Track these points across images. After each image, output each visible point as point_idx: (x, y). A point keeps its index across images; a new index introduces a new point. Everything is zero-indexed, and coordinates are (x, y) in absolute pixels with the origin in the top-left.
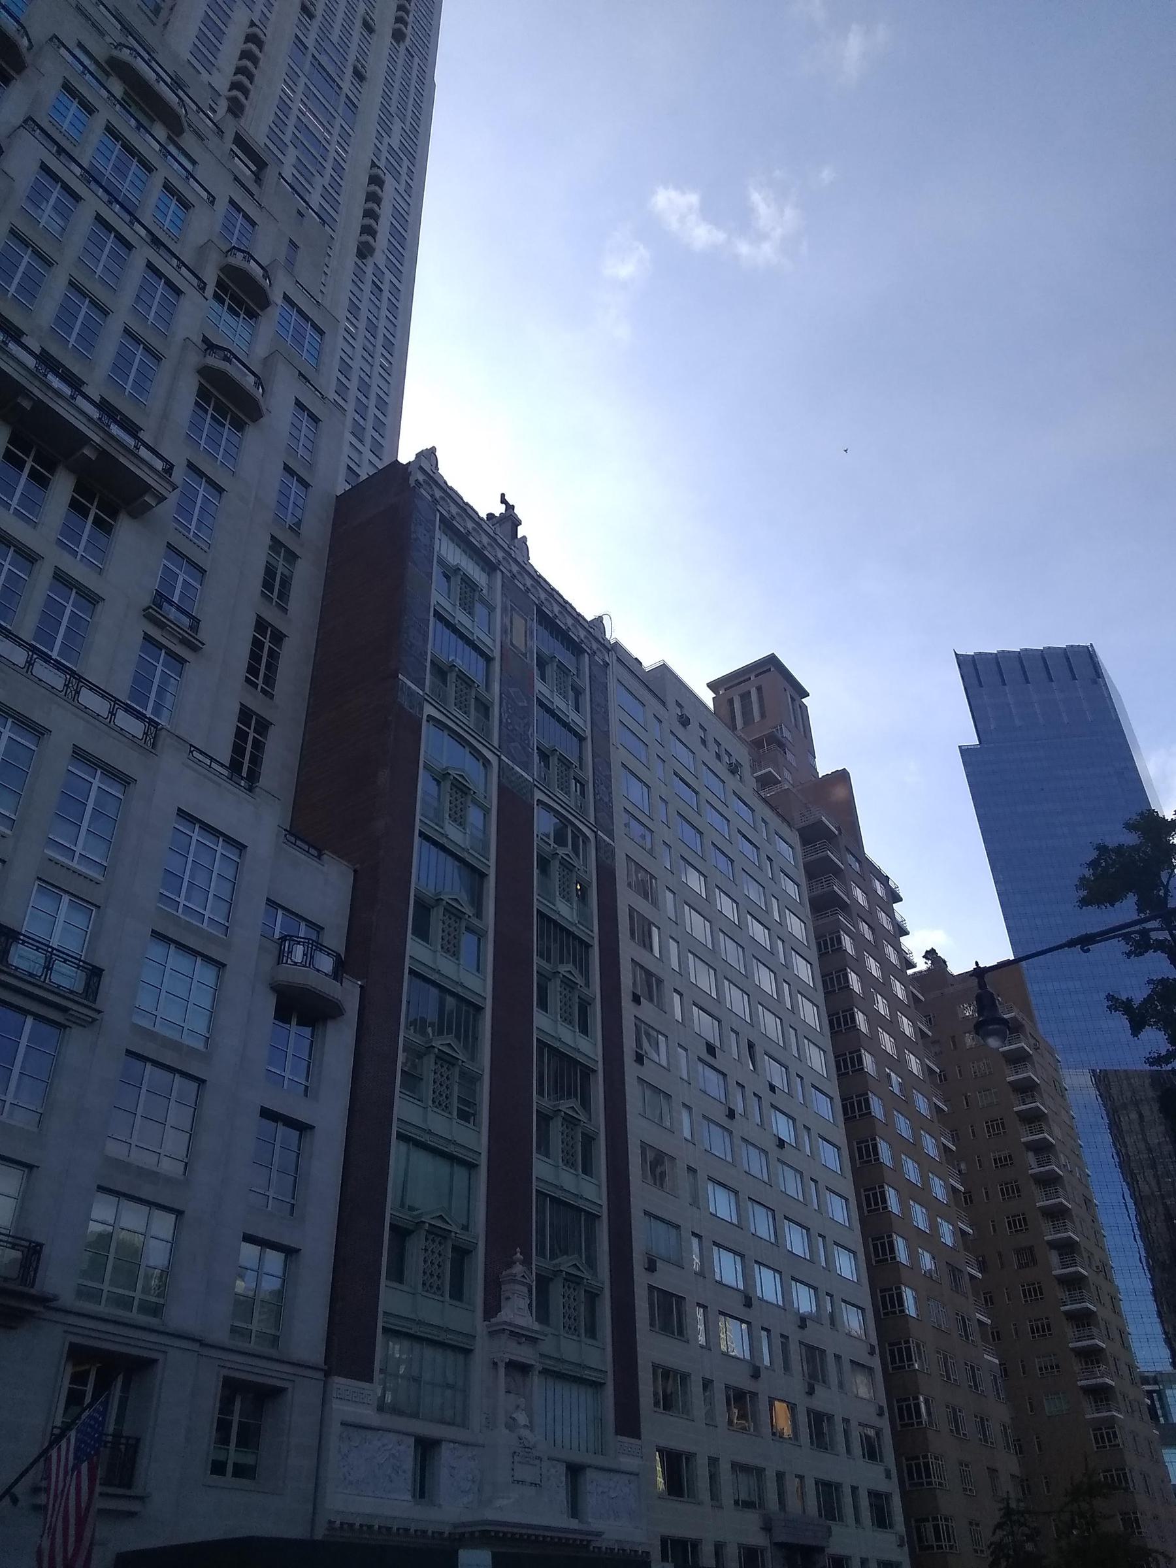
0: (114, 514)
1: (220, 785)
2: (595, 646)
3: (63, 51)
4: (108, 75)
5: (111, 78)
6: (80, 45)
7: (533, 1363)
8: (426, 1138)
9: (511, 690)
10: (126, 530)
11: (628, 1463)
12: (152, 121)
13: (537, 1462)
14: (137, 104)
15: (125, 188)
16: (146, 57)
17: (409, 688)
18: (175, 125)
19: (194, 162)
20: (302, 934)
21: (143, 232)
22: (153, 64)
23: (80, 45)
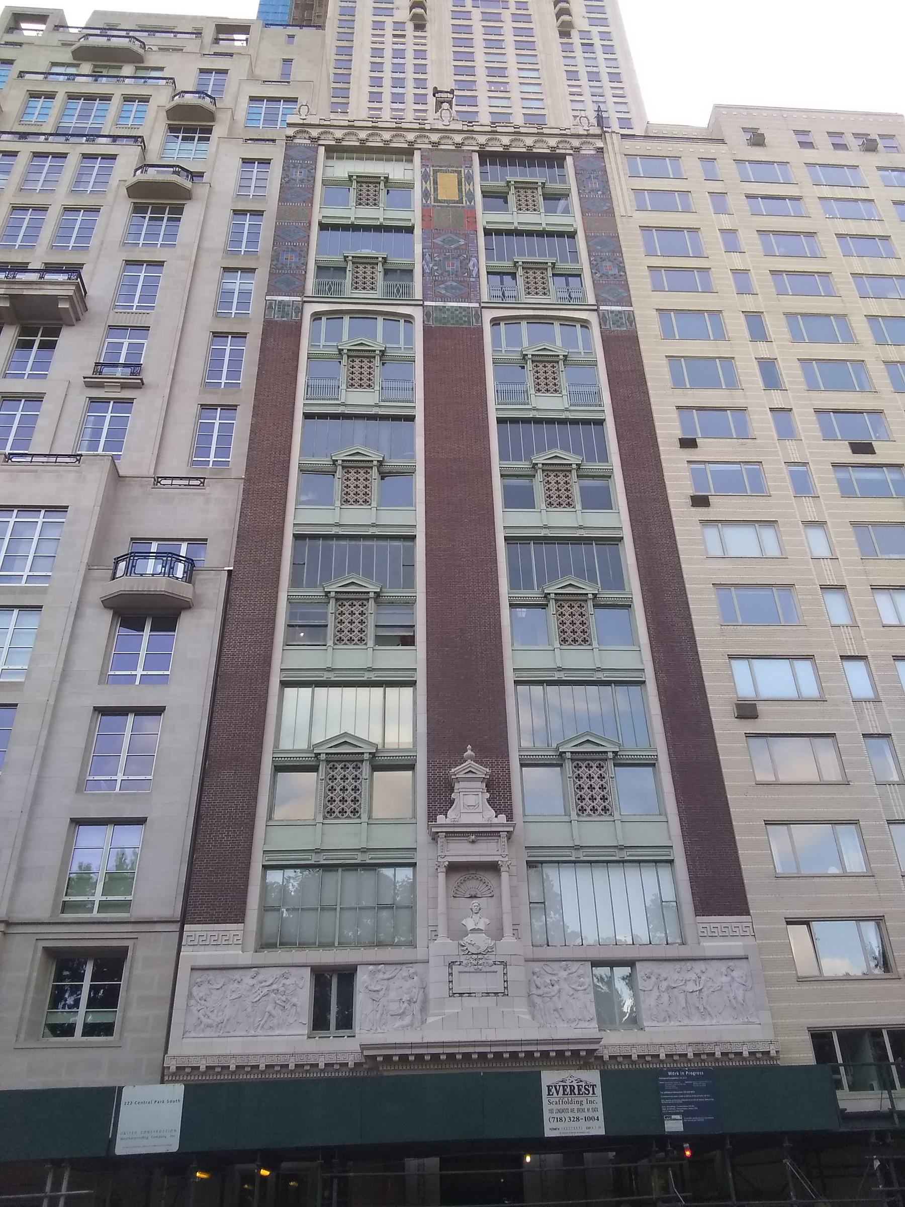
0: (56, 333)
1: (36, 471)
2: (576, 143)
3: (78, 79)
4: (77, 66)
5: (123, 68)
6: (54, 64)
7: (496, 859)
9: (438, 241)
10: (67, 339)
11: (711, 947)
12: (120, 68)
14: (105, 67)
15: (89, 125)
16: (131, 34)
17: (280, 302)
18: (134, 58)
19: (161, 69)
20: (183, 553)
21: (10, 137)
22: (124, 33)
23: (54, 64)
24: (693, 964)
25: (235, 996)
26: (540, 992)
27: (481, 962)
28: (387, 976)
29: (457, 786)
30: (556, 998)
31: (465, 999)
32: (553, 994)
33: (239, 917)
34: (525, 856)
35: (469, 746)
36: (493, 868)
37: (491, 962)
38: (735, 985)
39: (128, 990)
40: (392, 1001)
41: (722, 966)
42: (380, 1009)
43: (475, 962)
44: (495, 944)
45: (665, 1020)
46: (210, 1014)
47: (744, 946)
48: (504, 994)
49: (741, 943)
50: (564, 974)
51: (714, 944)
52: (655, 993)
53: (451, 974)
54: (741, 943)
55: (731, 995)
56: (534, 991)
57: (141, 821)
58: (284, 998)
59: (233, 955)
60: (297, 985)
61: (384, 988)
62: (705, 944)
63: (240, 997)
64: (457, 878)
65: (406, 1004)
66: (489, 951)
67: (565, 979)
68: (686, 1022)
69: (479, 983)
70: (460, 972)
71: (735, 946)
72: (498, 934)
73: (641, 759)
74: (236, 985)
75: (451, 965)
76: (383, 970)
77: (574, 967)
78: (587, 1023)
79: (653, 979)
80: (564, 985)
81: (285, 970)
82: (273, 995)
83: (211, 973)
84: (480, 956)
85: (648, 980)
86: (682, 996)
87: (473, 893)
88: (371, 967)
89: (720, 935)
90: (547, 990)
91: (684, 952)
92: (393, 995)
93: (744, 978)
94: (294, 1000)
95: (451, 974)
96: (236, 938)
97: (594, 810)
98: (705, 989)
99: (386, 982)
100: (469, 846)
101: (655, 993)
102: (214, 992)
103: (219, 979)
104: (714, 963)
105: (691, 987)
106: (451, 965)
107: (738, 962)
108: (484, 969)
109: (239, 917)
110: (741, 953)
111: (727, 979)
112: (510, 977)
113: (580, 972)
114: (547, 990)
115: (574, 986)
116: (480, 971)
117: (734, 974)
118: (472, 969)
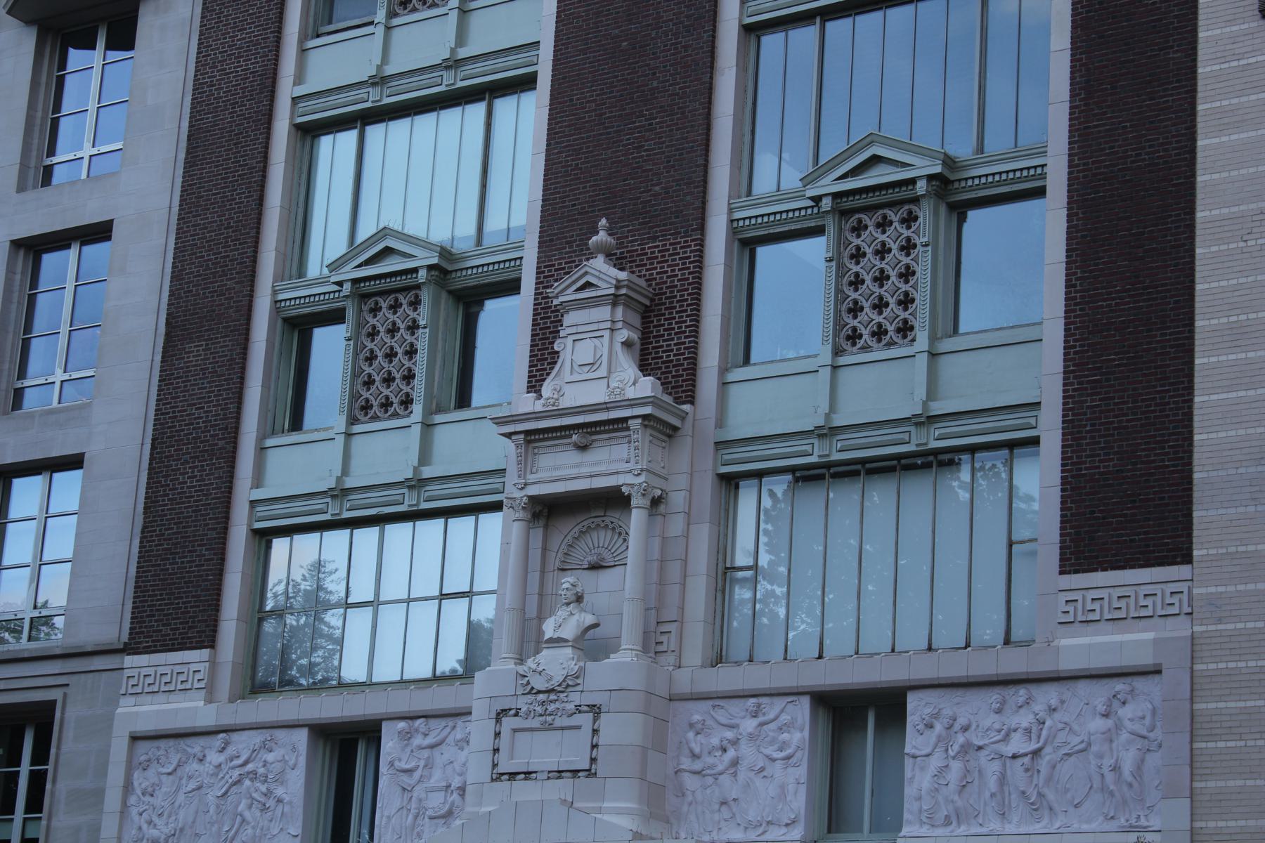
8: (374, 98)
13: (585, 720)
24: (1036, 690)
25: (192, 785)
26: (697, 766)
27: (552, 707)
28: (429, 740)
29: (569, 319)
30: (725, 779)
31: (519, 784)
32: (720, 768)
33: (207, 638)
34: (708, 467)
35: (603, 221)
36: (614, 500)
37: (570, 707)
38: (1124, 736)
39: (54, 781)
40: (433, 790)
41: (1098, 693)
42: (414, 805)
43: (539, 709)
44: (582, 669)
45: (947, 822)
46: (156, 819)
47: (1156, 641)
48: (590, 773)
49: (1150, 636)
50: (749, 725)
51: (1117, 638)
52: (936, 762)
53: (497, 735)
54: (1150, 636)
55: (1108, 762)
56: (686, 763)
57: (73, 462)
58: (263, 788)
59: (192, 709)
60: (286, 762)
61: (422, 763)
62: (1064, 642)
63: (199, 788)
64: (566, 529)
65: (455, 795)
66: (566, 686)
67: (751, 737)
68: (995, 825)
69: (545, 751)
70: (515, 731)
71: (1132, 643)
72: (592, 644)
73: (1020, 180)
74: (195, 766)
75: (501, 714)
76: (423, 729)
77: (773, 707)
78: (784, 830)
79: (938, 727)
80: (746, 750)
81: (266, 734)
82: (247, 782)
83: (163, 744)
84: (552, 697)
85: (928, 732)
86: (996, 766)
87: (592, 559)
88: (402, 725)
89: (1124, 615)
90: (710, 760)
91: (1013, 662)
92: (437, 778)
93: (1148, 721)
94: (279, 791)
95: (497, 735)
96: (198, 676)
97: (879, 333)
98: (1048, 749)
99: (426, 753)
100: (573, 457)
101: (936, 762)
102: (164, 778)
103: (171, 753)
104: (1083, 687)
105: (1017, 744)
106: (501, 714)
107: (1139, 683)
108: (559, 722)
109: (207, 638)
110: (1144, 659)
111: (1109, 723)
112: (602, 739)
113: (785, 718)
114: (710, 760)
115: (769, 751)
116: (549, 727)
117: (1121, 712)
118: (535, 723)
